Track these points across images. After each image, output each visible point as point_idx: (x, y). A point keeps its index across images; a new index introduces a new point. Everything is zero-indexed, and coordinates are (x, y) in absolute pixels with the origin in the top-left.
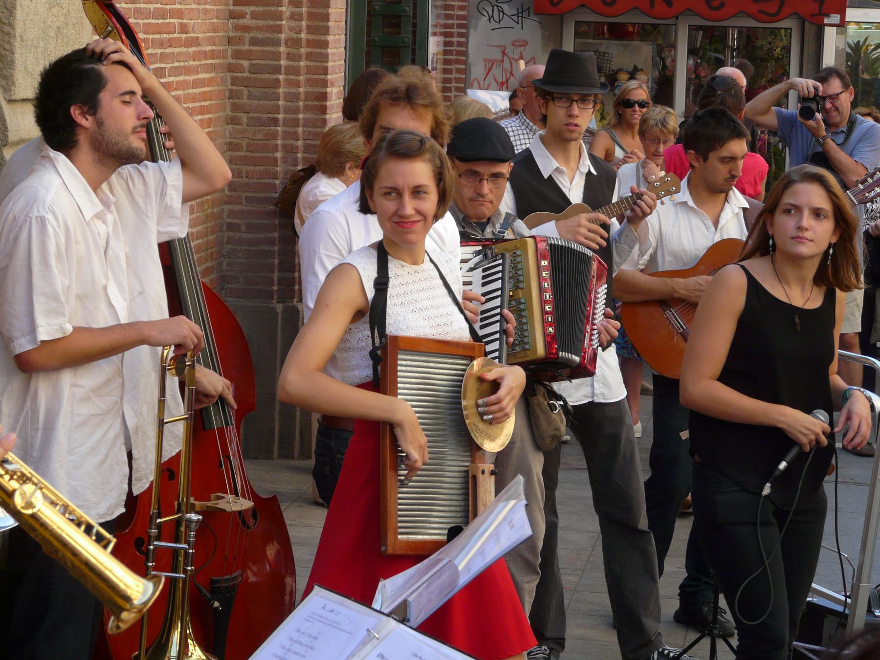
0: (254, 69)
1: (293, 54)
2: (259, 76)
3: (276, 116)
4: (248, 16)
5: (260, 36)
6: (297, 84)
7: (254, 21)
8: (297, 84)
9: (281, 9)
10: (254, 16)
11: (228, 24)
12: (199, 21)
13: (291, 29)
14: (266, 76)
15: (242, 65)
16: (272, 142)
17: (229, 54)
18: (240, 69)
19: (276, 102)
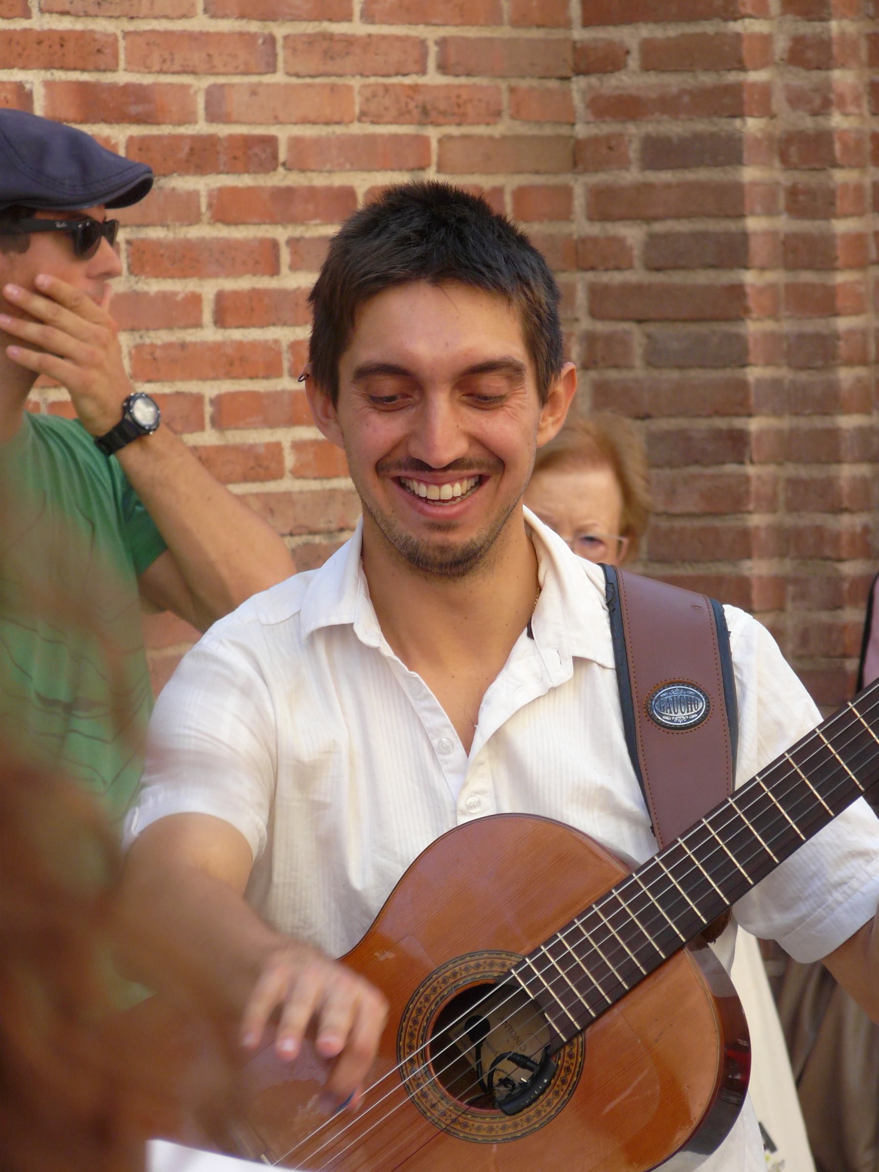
0: (664, 255)
1: (810, 192)
2: (677, 278)
3: (739, 423)
4: (633, 62)
5: (675, 128)
6: (826, 303)
7: (653, 79)
8: (826, 303)
9: (736, 26)
10: (654, 58)
11: (567, 95)
12: (279, 78)
13: (796, 99)
14: (702, 278)
15: (619, 241)
16: (730, 522)
17: (579, 203)
18: (612, 255)
19: (737, 373)
